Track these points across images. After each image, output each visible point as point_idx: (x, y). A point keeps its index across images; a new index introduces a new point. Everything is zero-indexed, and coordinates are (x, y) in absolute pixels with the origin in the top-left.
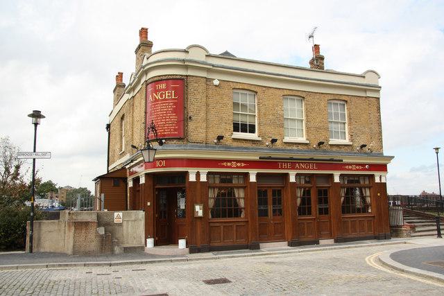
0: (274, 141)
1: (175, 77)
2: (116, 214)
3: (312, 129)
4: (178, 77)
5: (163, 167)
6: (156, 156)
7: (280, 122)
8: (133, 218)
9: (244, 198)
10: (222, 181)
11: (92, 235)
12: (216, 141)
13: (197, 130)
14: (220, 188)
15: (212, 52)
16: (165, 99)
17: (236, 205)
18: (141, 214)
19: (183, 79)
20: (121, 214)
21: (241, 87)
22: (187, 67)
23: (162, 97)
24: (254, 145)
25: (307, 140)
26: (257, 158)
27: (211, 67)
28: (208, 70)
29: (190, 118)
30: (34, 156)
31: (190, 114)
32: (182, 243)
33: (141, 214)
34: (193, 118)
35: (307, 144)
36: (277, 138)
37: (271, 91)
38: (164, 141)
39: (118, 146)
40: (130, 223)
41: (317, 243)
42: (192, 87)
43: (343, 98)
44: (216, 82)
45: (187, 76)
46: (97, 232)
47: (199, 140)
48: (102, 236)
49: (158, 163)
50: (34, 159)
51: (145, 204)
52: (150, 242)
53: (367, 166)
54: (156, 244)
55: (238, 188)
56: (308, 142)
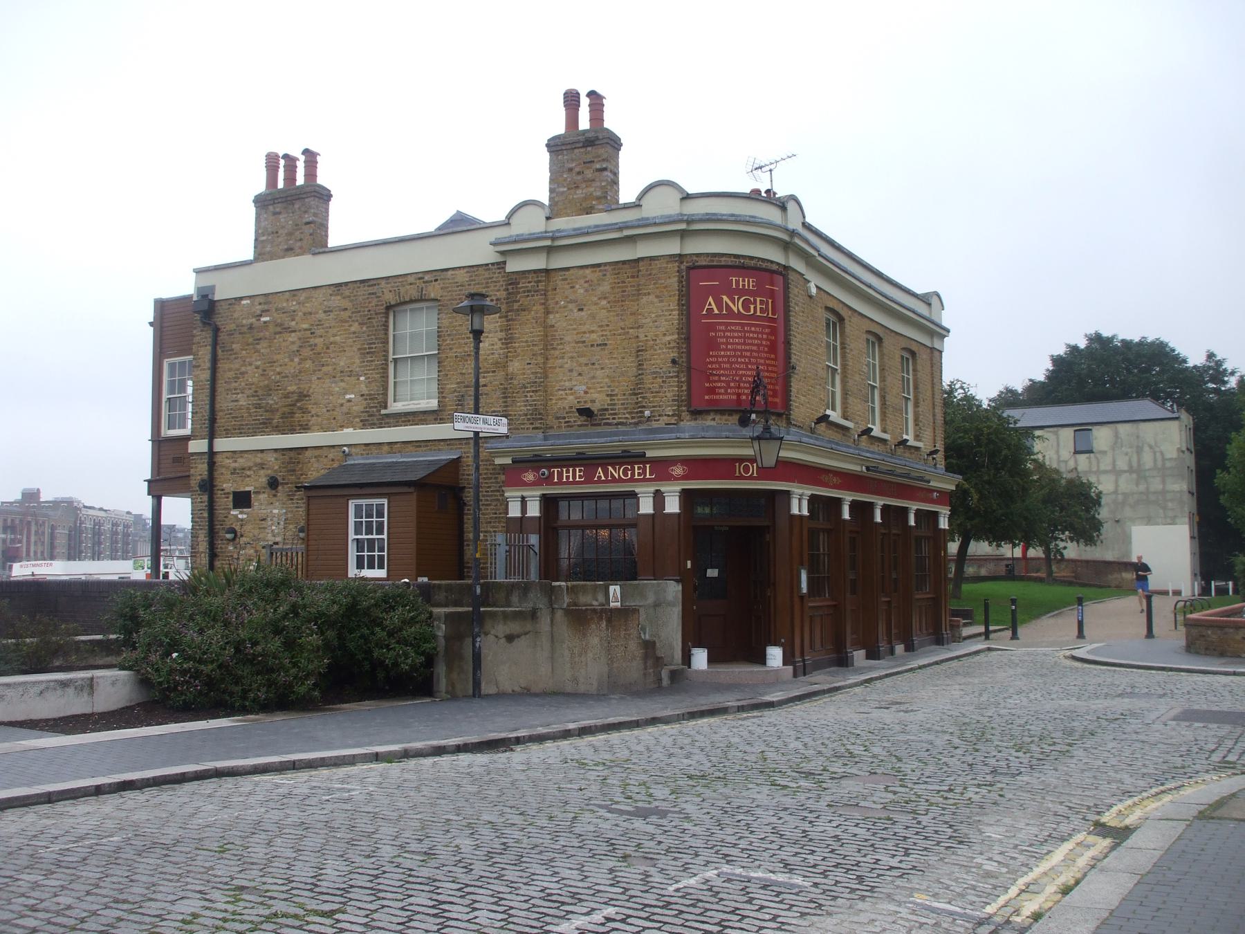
5: (751, 478)
6: (783, 454)
8: (651, 599)
11: (633, 645)
16: (753, 317)
22: (786, 246)
23: (746, 308)
25: (884, 431)
32: (775, 655)
33: (673, 590)
37: (856, 319)
41: (892, 652)
43: (914, 348)
44: (814, 291)
45: (786, 268)
49: (740, 469)
52: (700, 658)
54: (711, 660)
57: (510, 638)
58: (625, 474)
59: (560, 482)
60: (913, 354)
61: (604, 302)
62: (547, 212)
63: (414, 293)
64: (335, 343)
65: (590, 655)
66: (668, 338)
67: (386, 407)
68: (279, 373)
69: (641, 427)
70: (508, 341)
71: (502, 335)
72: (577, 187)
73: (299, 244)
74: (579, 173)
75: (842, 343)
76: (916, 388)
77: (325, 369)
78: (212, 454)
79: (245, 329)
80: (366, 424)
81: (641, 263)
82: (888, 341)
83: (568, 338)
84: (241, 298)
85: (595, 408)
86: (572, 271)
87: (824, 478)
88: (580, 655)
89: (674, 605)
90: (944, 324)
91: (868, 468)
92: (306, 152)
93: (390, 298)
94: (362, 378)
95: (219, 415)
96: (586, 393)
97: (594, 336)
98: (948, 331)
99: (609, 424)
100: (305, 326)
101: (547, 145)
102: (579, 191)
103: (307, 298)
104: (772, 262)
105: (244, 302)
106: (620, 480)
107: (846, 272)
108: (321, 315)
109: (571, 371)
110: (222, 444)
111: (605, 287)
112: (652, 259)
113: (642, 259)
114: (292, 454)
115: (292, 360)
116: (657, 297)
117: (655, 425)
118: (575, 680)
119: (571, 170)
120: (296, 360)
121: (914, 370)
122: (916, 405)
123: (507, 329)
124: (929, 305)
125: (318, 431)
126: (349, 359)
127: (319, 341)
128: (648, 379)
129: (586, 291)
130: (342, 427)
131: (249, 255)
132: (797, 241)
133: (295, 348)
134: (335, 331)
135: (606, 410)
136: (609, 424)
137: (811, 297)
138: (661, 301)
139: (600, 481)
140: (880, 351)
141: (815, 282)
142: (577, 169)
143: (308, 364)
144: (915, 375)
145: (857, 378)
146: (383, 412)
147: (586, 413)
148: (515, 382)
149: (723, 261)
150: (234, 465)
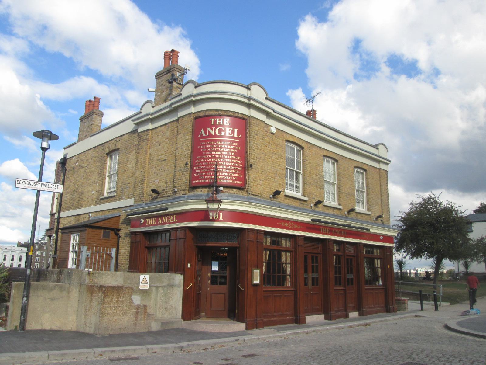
0: (319, 202)
1: (236, 115)
2: (142, 276)
3: (344, 194)
4: (240, 115)
7: (320, 184)
8: (165, 284)
9: (290, 264)
10: (273, 243)
12: (271, 196)
13: (258, 182)
14: (270, 250)
15: (270, 97)
17: (284, 271)
18: (179, 278)
19: (244, 119)
20: (147, 277)
21: (292, 140)
22: (249, 106)
24: (301, 205)
25: (339, 205)
26: (309, 220)
27: (272, 111)
28: (268, 115)
29: (251, 166)
30: (39, 187)
31: (252, 161)
33: (179, 278)
34: (254, 166)
35: (340, 209)
36: (321, 200)
37: (315, 149)
38: (221, 189)
39: (97, 187)
40: (160, 289)
41: (347, 316)
42: (254, 129)
43: (365, 167)
44: (274, 130)
45: (249, 117)
46: (131, 302)
47: (257, 193)
48: (138, 307)
50: (39, 191)
51: (185, 266)
53: (381, 237)
55: (286, 251)
56: (341, 207)
57: (53, 299)
58: (168, 221)
59: (149, 226)
60: (365, 170)
61: (167, 140)
62: (153, 104)
63: (113, 147)
64: (92, 171)
65: (93, 311)
66: (186, 153)
67: (103, 195)
68: (78, 185)
69: (175, 196)
70: (137, 162)
71: (135, 160)
72: (163, 92)
73: (88, 133)
74: (164, 86)
75: (303, 160)
76: (367, 186)
77: (89, 182)
78: (59, 218)
79: (72, 169)
80: (97, 204)
81: (179, 120)
82: (341, 162)
83: (155, 159)
84: (73, 157)
85: (159, 190)
86: (159, 128)
87: (282, 224)
88: (89, 311)
89: (179, 287)
90: (388, 158)
91: (312, 220)
92: (95, 98)
93: (107, 150)
94: (97, 184)
95: (63, 203)
96: (158, 183)
97: (163, 156)
98: (390, 161)
99: (164, 197)
100: (86, 165)
101: (156, 76)
102: (164, 93)
103: (88, 154)
104: (238, 113)
105: (74, 158)
106: (166, 223)
107: (301, 124)
108: (90, 160)
109: (155, 173)
110: (62, 215)
111: (168, 134)
112: (183, 117)
113: (180, 118)
114: (77, 217)
115: (81, 179)
116: (183, 134)
117: (178, 195)
118: (85, 324)
119: (162, 85)
120: (82, 179)
121: (366, 178)
122: (368, 194)
123: (137, 158)
124: (378, 149)
125: (84, 207)
126: (94, 177)
127: (88, 171)
128: (177, 173)
129: (162, 136)
130: (90, 205)
131: (75, 139)
132: (252, 102)
133: (82, 174)
134: (92, 166)
135: (164, 190)
136: (164, 197)
137: (273, 134)
138: (184, 136)
139: (160, 224)
140: (337, 166)
141: (274, 126)
142: (164, 84)
143: (85, 180)
144: (366, 180)
145: (315, 177)
146: (101, 197)
147: (154, 191)
148: (137, 180)
149: (210, 113)
150: (64, 223)
